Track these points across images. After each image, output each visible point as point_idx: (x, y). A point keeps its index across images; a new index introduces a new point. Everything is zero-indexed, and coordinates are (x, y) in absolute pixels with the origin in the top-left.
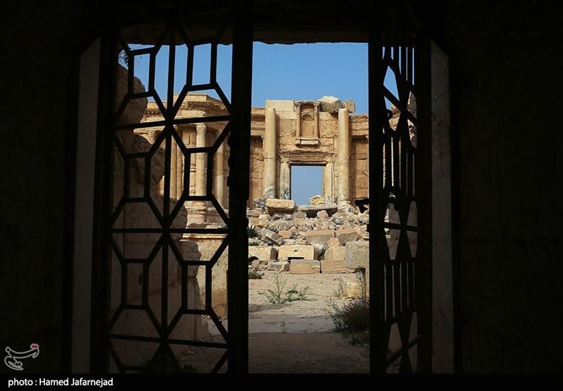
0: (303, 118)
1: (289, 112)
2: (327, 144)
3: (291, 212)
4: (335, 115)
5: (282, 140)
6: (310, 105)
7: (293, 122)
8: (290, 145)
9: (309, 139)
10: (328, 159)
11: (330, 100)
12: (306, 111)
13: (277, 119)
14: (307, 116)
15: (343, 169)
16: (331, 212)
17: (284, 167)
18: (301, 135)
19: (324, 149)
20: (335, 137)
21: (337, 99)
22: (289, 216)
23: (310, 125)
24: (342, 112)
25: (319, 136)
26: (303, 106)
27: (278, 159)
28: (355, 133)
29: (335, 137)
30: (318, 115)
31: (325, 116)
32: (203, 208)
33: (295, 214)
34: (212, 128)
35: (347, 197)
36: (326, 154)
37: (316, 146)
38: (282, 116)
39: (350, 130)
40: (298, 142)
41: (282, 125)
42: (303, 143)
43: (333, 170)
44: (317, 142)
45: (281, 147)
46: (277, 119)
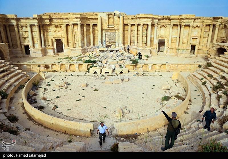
0: (109, 18)
1: (105, 17)
2: (116, 26)
3: (106, 51)
4: (119, 17)
5: (103, 26)
6: (111, 14)
7: (106, 20)
8: (105, 27)
9: (111, 25)
10: (117, 31)
11: (117, 12)
12: (110, 16)
13: (101, 19)
14: (110, 17)
15: (121, 35)
16: (117, 51)
17: (104, 34)
18: (109, 24)
19: (115, 28)
20: (119, 24)
21: (119, 13)
22: (105, 52)
23: (111, 20)
24: (121, 17)
25: (114, 24)
26: (109, 15)
27: (102, 31)
28: (125, 23)
29: (119, 24)
30: (114, 17)
31: (116, 17)
32: (82, 48)
33: (107, 52)
35: (122, 43)
36: (116, 30)
37: (113, 27)
38: (103, 18)
39: (123, 22)
40: (108, 26)
41: (103, 21)
42: (109, 26)
43: (118, 34)
44: (113, 26)
45: (103, 28)
46: (101, 19)
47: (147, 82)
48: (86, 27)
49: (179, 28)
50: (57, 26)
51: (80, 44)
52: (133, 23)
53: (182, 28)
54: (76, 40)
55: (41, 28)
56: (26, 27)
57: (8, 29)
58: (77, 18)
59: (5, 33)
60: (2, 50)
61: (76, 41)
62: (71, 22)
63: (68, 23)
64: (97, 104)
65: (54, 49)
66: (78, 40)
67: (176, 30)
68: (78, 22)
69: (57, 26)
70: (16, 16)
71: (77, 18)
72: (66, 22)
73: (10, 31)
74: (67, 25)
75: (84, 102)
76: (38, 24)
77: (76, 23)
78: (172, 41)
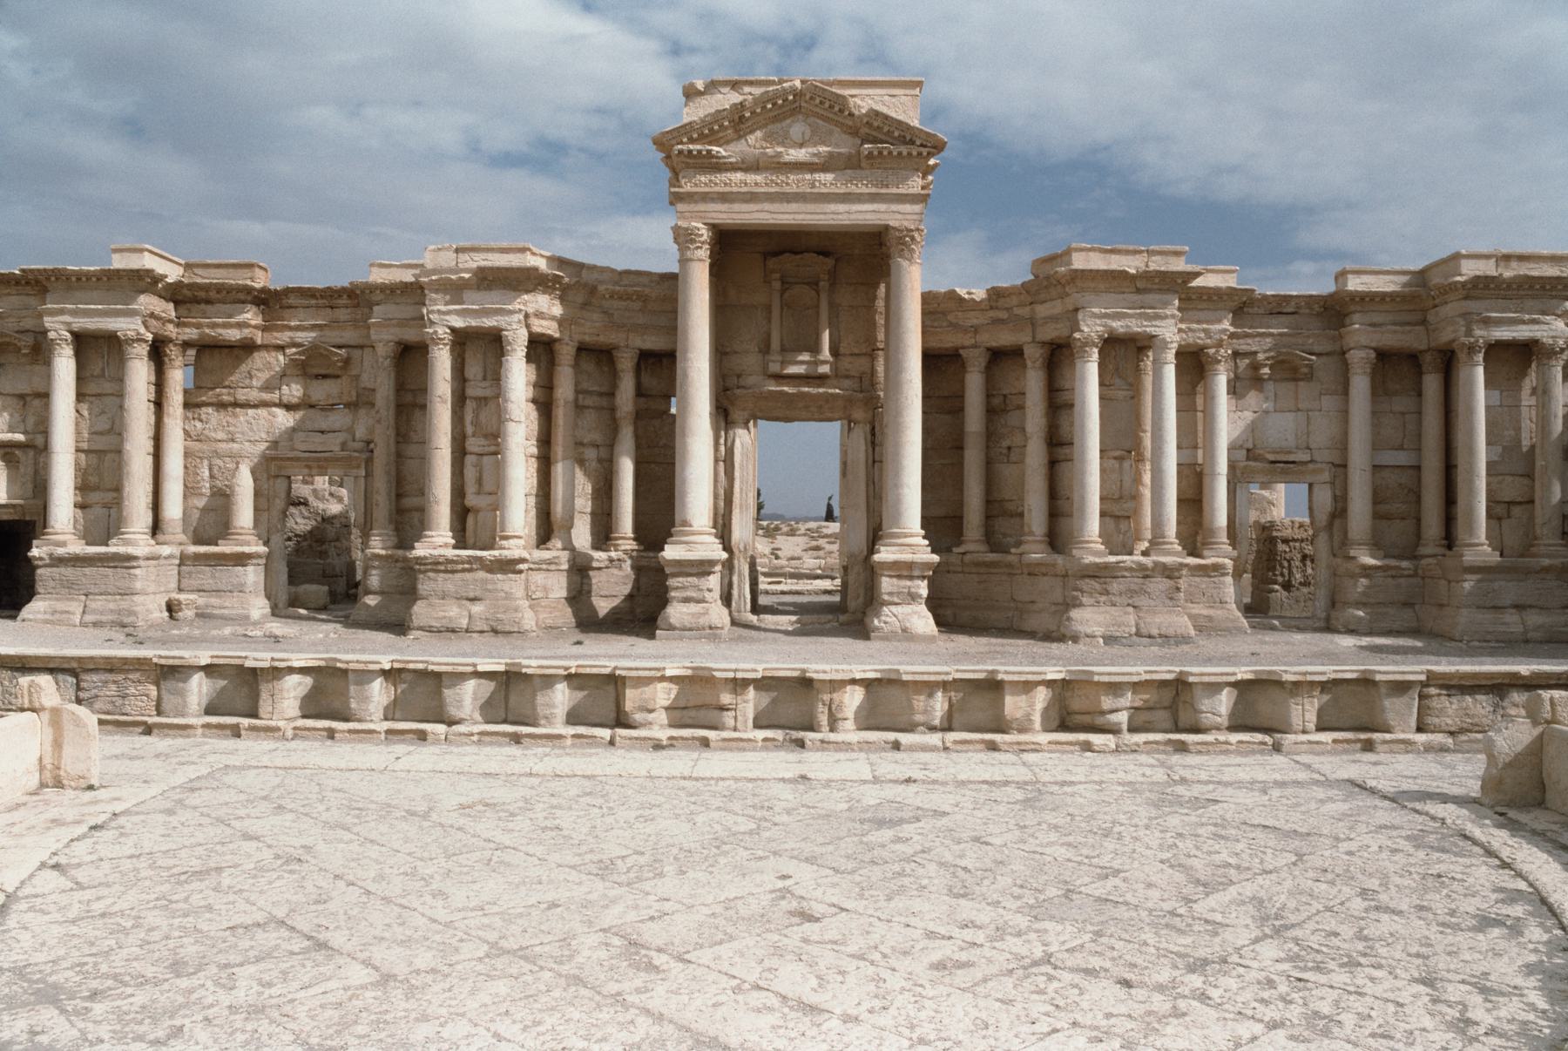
34: (543, 335)
47: (1215, 825)
48: (576, 365)
49: (1432, 384)
52: (1004, 338)
54: (480, 481)
61: (470, 488)
62: (444, 318)
63: (410, 335)
64: (647, 1012)
67: (1402, 403)
75: (472, 993)
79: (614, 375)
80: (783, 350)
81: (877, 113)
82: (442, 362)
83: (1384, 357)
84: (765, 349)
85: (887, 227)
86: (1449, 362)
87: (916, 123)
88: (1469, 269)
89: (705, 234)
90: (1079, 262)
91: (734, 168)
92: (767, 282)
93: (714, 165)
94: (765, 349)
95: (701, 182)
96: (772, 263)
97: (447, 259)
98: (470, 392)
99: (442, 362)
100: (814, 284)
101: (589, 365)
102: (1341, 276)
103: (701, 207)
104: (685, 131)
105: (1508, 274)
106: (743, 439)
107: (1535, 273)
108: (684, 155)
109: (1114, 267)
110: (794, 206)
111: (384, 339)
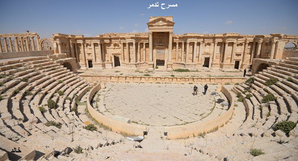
49: (223, 45)
50: (115, 45)
51: (135, 60)
53: (227, 45)
55: (103, 46)
56: (90, 45)
57: (76, 47)
58: (132, 38)
59: (74, 49)
60: (71, 64)
62: (128, 41)
65: (112, 63)
66: (133, 56)
68: (134, 41)
69: (115, 45)
70: (83, 36)
71: (132, 38)
72: (123, 41)
73: (77, 48)
74: (124, 44)
76: (100, 42)
77: (131, 42)
78: (216, 57)
79: (143, 45)
80: (159, 43)
81: (168, 20)
82: (127, 45)
83: (218, 42)
84: (157, 43)
85: (169, 32)
86: (225, 44)
87: (172, 21)
88: (227, 35)
89: (152, 33)
90: (188, 35)
91: (154, 26)
92: (158, 36)
93: (152, 26)
94: (157, 43)
95: (150, 28)
96: (158, 34)
97: (128, 36)
98: (130, 48)
99: (127, 45)
100: (162, 36)
101: (141, 44)
102: (215, 35)
103: (152, 30)
104: (150, 23)
105: (231, 36)
106: (155, 51)
107: (234, 36)
108: (150, 25)
109: (191, 36)
110: (160, 30)
111: (122, 42)
